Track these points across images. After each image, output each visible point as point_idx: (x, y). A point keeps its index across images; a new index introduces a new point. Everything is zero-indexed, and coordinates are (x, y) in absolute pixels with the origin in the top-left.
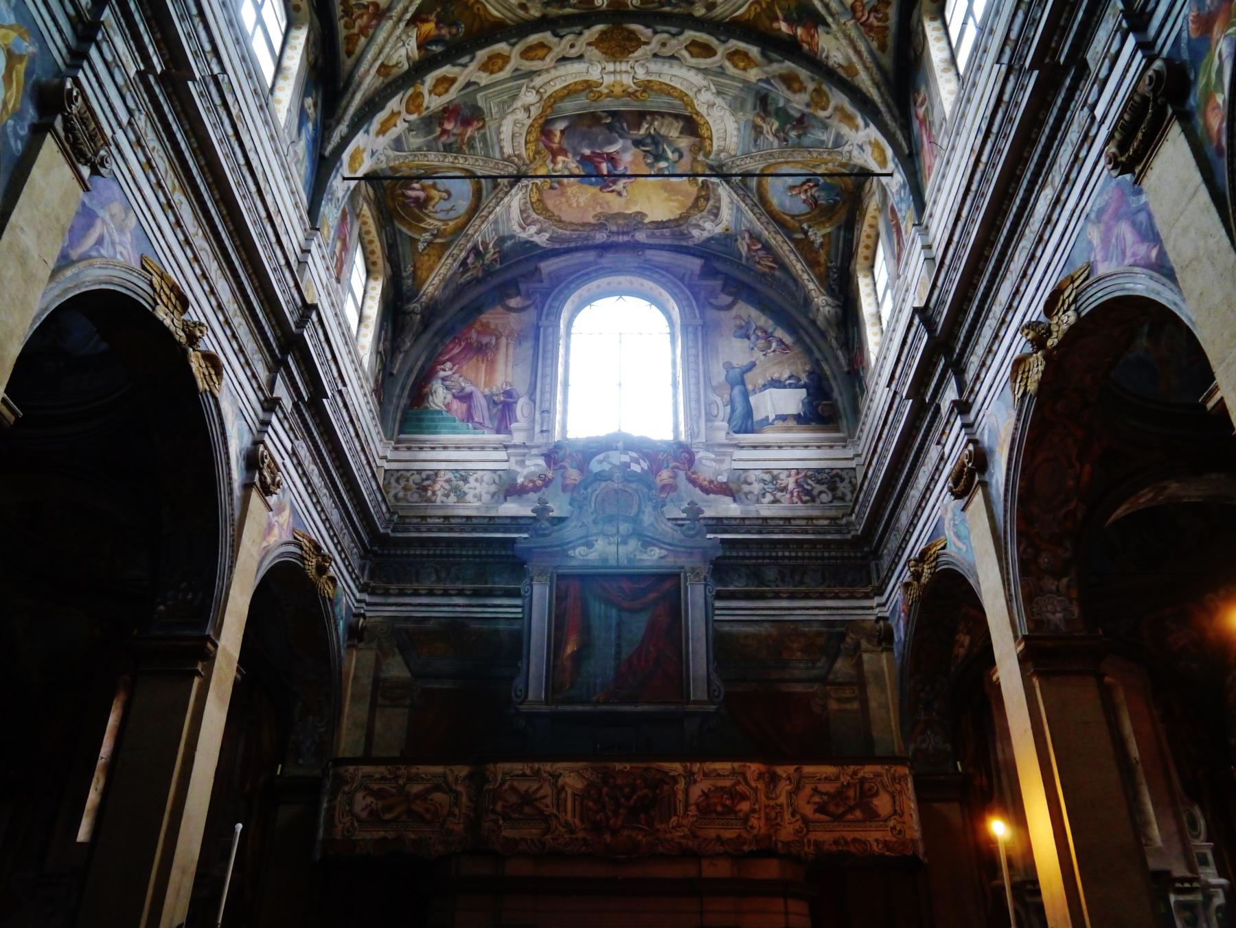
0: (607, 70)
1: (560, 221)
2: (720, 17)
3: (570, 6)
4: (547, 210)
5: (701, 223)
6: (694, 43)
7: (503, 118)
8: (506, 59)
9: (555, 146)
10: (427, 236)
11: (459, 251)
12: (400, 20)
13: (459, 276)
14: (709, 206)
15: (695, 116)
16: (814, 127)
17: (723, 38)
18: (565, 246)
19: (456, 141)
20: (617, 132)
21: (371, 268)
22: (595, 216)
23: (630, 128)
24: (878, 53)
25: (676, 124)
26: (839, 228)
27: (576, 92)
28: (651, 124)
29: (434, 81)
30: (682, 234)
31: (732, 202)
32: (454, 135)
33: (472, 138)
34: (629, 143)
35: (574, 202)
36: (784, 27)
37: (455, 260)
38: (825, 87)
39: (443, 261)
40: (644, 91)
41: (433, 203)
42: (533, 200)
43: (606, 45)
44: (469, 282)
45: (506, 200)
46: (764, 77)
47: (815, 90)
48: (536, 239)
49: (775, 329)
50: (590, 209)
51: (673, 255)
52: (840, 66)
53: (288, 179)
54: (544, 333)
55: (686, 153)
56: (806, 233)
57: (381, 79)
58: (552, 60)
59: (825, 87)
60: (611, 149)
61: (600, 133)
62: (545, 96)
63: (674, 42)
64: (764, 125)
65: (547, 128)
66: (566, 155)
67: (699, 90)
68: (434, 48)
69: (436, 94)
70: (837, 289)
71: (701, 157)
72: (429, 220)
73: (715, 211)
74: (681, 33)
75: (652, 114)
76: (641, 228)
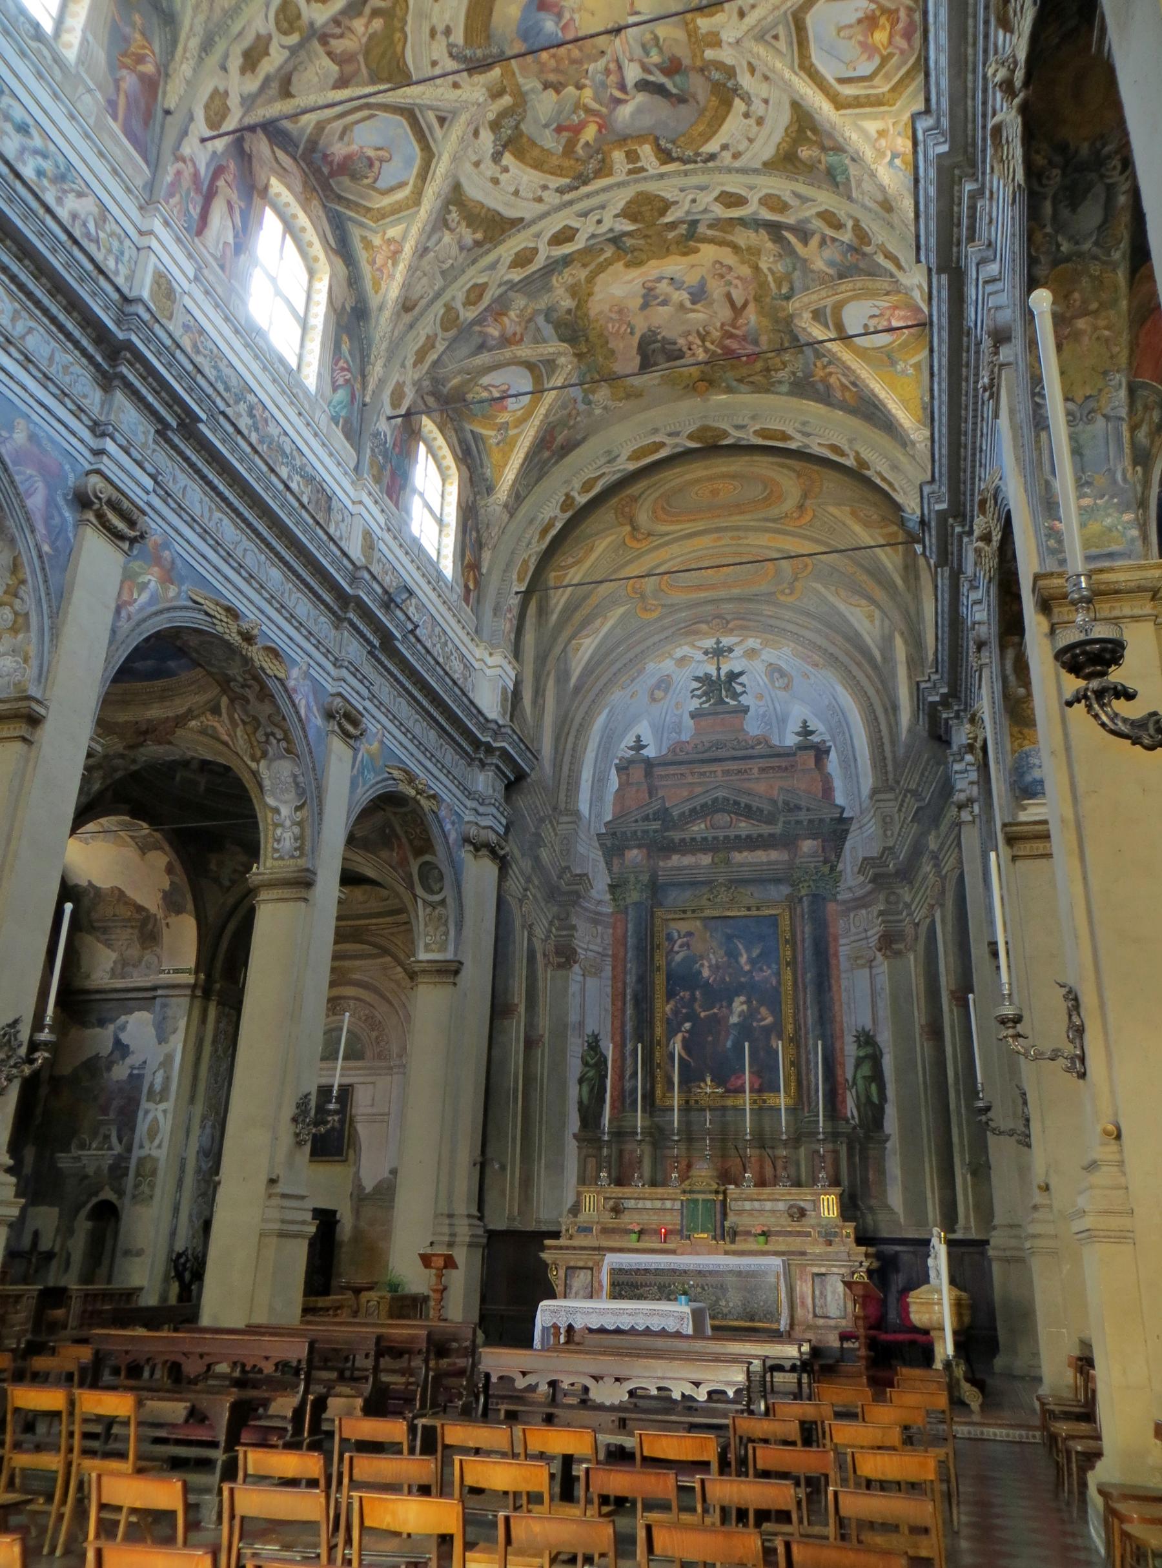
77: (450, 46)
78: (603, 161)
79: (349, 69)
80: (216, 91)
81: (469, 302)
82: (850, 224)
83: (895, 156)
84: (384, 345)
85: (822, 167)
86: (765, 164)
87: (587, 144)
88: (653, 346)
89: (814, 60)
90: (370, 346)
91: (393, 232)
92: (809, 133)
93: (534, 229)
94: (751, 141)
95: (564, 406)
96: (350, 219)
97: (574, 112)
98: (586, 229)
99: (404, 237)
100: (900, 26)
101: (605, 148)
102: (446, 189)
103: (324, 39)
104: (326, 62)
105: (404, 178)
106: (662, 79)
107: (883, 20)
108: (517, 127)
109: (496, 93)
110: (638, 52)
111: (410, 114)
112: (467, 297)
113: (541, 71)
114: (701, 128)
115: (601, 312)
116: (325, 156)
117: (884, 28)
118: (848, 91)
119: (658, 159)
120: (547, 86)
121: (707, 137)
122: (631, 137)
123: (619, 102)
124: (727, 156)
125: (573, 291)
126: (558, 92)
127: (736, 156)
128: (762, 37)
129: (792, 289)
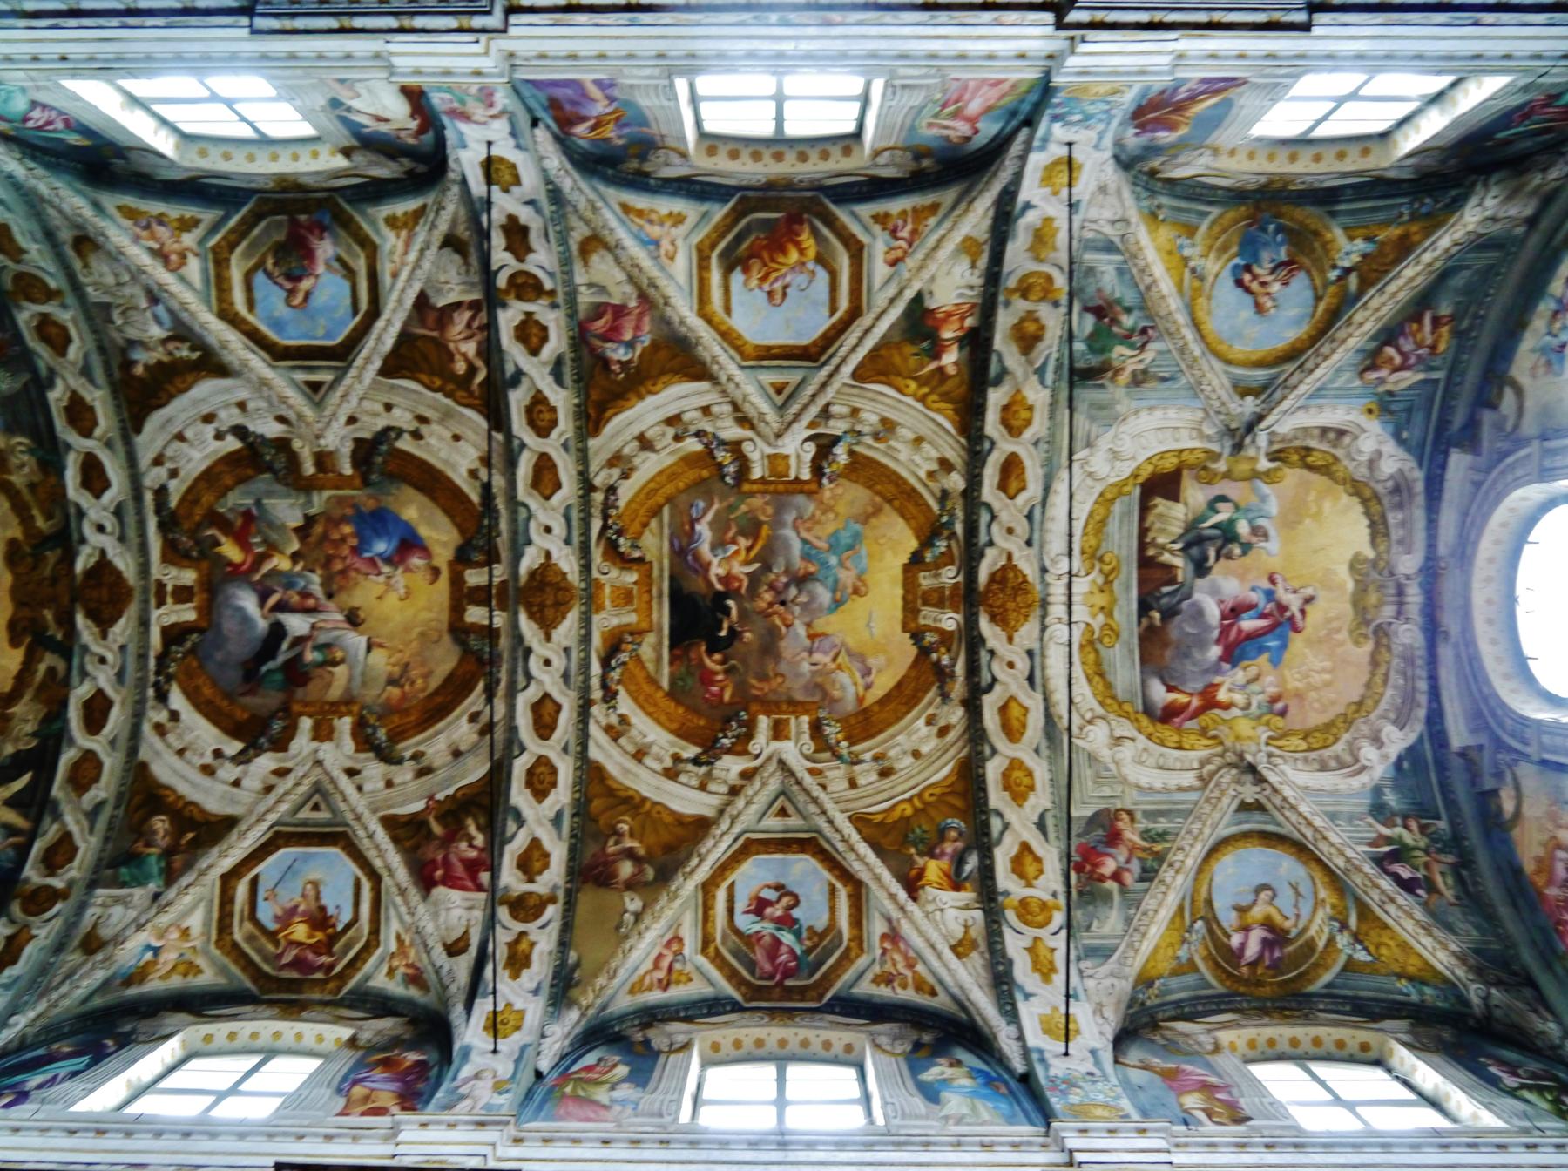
1: (1360, 704)
2: (963, 453)
3: (954, 665)
4: (1328, 727)
5: (1364, 458)
6: (1003, 486)
7: (1124, 781)
8: (1015, 764)
9: (1196, 702)
10: (1343, 940)
11: (1379, 888)
12: (902, 909)
14: (1325, 447)
15: (1140, 480)
16: (1099, 290)
17: (987, 445)
18: (1423, 699)
19: (1140, 859)
20: (1180, 602)
21: (1372, 1055)
22: (1357, 643)
23: (1172, 581)
24: (942, 212)
25: (1160, 509)
26: (1333, 214)
27: (1098, 663)
28: (1163, 548)
29: (1015, 877)
30: (1397, 490)
32: (1128, 862)
33: (1146, 835)
34: (1200, 582)
35: (1316, 679)
36: (950, 358)
37: (1392, 900)
38: (1012, 283)
39: (1390, 922)
40: (1101, 560)
41: (1278, 919)
42: (1304, 746)
44: (1460, 881)
45: (1288, 792)
46: (1034, 378)
49: (1552, 296)
50: (1339, 650)
52: (973, 266)
53: (927, 1144)
55: (1217, 490)
56: (1348, 271)
57: (975, 955)
58: (1030, 697)
59: (1012, 283)
60: (1213, 613)
61: (1180, 628)
62: (1100, 710)
63: (1004, 516)
65: (1159, 713)
66: (1217, 686)
67: (1090, 474)
68: (968, 868)
69: (1036, 878)
70: (1453, 193)
71: (1221, 466)
72: (1312, 932)
73: (1332, 435)
75: (1142, 547)
76: (1388, 563)
77: (400, 432)
79: (431, 318)
80: (517, 181)
81: (45, 323)
82: (57, 883)
83: (156, 951)
84: (43, 189)
85: (140, 847)
86: (144, 767)
87: (219, 544)
89: (283, 851)
90: (47, 166)
91: (194, 268)
92: (190, 835)
93: (119, 445)
98: (97, 510)
99: (183, 280)
100: (310, 956)
101: (205, 565)
102: (228, 358)
103: (474, 306)
104: (452, 298)
105: (259, 308)
107: (320, 936)
108: (269, 468)
110: (322, 638)
111: (343, 353)
112: (55, 324)
114: (207, 691)
117: (310, 937)
118: (242, 890)
119: (174, 625)
120: (310, 521)
121: (193, 696)
123: (263, 600)
124: (162, 716)
126: (297, 530)
127: (160, 729)
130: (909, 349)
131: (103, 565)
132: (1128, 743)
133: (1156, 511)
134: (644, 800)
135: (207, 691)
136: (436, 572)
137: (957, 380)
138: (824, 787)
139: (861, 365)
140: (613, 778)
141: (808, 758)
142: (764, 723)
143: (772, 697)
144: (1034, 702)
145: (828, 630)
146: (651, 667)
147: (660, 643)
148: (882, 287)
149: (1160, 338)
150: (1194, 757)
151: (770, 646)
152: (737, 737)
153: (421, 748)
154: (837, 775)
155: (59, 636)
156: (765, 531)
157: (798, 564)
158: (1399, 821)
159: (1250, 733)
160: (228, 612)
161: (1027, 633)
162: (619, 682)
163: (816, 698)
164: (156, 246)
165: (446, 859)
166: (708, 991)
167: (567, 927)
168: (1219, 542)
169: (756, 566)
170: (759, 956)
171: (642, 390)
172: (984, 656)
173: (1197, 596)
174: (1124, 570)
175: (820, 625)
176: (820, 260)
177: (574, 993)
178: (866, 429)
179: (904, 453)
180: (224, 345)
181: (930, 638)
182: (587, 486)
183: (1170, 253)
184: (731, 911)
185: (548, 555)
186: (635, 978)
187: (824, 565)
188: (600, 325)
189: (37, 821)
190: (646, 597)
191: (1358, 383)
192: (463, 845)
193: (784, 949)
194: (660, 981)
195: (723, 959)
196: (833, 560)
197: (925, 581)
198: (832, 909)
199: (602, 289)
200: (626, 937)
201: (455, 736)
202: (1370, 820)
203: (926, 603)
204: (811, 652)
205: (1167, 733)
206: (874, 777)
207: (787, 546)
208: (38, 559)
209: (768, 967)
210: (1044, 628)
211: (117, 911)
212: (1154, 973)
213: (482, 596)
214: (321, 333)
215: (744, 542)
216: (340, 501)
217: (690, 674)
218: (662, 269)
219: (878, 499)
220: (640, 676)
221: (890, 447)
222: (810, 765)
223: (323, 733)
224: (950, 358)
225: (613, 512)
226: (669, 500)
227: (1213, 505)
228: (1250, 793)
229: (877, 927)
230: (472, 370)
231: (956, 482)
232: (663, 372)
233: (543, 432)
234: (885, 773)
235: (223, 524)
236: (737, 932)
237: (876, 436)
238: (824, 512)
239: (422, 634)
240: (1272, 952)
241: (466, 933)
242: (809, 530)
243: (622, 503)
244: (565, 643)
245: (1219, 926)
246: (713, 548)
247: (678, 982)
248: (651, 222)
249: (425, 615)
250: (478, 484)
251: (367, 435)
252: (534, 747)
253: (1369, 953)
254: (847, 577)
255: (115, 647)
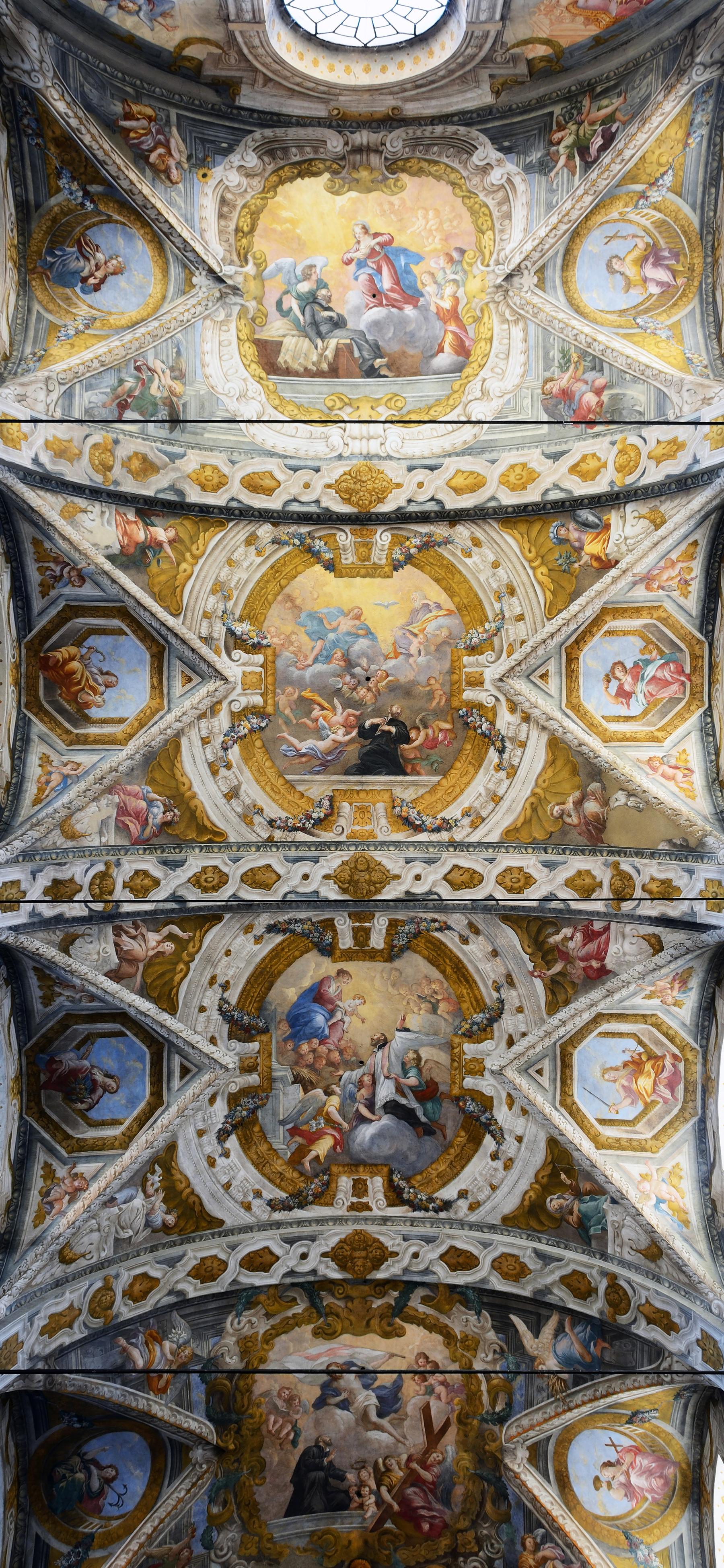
0: (379, 441)
2: (241, 526)
5: (245, 181)
7: (518, 386)
8: (504, 480)
9: (452, 327)
13: (619, 115)
14: (235, 215)
15: (263, 375)
16: (104, 406)
17: (234, 504)
18: (451, 129)
20: (367, 341)
22: (402, 188)
23: (349, 347)
24: (40, 537)
30: (271, 153)
31: (202, 232)
32: (586, 383)
33: (563, 368)
34: (350, 325)
35: (433, 223)
39: (639, 154)
41: (636, 253)
42: (490, 233)
43: (378, 484)
44: (605, 92)
45: (529, 246)
47: (110, 468)
48: (494, 155)
51: (285, 110)
54: (494, 12)
55: (272, 309)
56: (86, 194)
60: (377, 313)
64: (171, 383)
65: (461, 358)
68: (591, 518)
69: (599, 459)
70: (19, 98)
71: (252, 305)
72: (648, 224)
73: (225, 209)
74: (287, 503)
75: (320, 374)
76: (334, 161)
77: (223, 1000)
78: (327, 1184)
79: (127, 969)
80: (16, 883)
82: (603, 1285)
83: (660, 1201)
85: (573, 1219)
86: (505, 1219)
87: (317, 1157)
88: (313, 1475)
92: (563, 1176)
93: (232, 1239)
94: (494, 1188)
95: (176, 1536)
96: (43, 1141)
97: (315, 1118)
99: (95, 1177)
100: (665, 1074)
101: (335, 1169)
102: (161, 1141)
103: (118, 931)
104: (111, 950)
105: (120, 1117)
106: (414, 1105)
107: (648, 1067)
108: (253, 1111)
109: (247, 1068)
110: (398, 1070)
112: (131, 1285)
113: (297, 1063)
114: (442, 1167)
115: (266, 1394)
116: (52, 1061)
117: (649, 1075)
120: (297, 1080)
121: (445, 1180)
122: (365, 1164)
123: (363, 1120)
124: (463, 1204)
125: (246, 1346)
126: (306, 1091)
127: (472, 1208)
128: (526, 1070)
129: (509, 1405)
130: (154, 568)
131: (336, 1255)
132: (487, 384)
133: (290, 361)
134: (533, 794)
135: (442, 1167)
136: (341, 973)
137: (179, 528)
138: (523, 642)
139: (166, 608)
140: (517, 819)
141: (498, 658)
142: (469, 694)
143: (447, 688)
144: (452, 465)
145: (391, 640)
146: (422, 791)
147: (401, 782)
148: (103, 590)
149: (143, 355)
150: (498, 328)
151: (405, 691)
152: (481, 716)
153: (490, 983)
154: (514, 631)
155: (396, 1294)
156: (307, 694)
157: (336, 665)
158: (554, 148)
159: (478, 279)
160: (375, 1150)
161: (394, 471)
162: (435, 818)
163: (449, 650)
164: (67, 1197)
165: (583, 959)
166: (695, 737)
167: (639, 853)
168: (317, 308)
169: (336, 701)
170: (666, 694)
171: (188, 794)
172: (413, 508)
173: (362, 327)
174: (340, 389)
175: (386, 647)
176: (79, 644)
177: (692, 843)
178: (221, 607)
179: (241, 575)
180: (150, 1145)
181: (398, 555)
182: (269, 843)
183: (72, 346)
184: (628, 719)
185: (327, 877)
186: (682, 795)
187: (335, 644)
188: (134, 828)
189: (551, 1307)
190: (362, 795)
191: (180, 185)
192: (571, 944)
193: (659, 674)
194: (685, 776)
195: (667, 724)
196: (332, 636)
197: (349, 558)
198: (626, 633)
199: (104, 823)
200: (647, 802)
201: (480, 955)
202: (552, 174)
203: (368, 559)
204: (411, 655)
205: (477, 351)
206: (515, 599)
207: (320, 674)
208: (330, 1312)
209: (675, 687)
210: (390, 457)
211: (626, 1233)
212: (680, 358)
213: (361, 935)
214: (139, 1065)
215: (317, 712)
216: (281, 1053)
217: (427, 758)
218: (87, 773)
219: (279, 598)
220: (429, 799)
221: (236, 588)
222: (504, 655)
223: (477, 1068)
224: (161, 533)
225: (291, 823)
226: (281, 775)
227: (285, 313)
228: (528, 280)
229: (641, 593)
230: (171, 937)
231: (265, 531)
232: (173, 776)
233: (223, 879)
234: (512, 592)
235: (300, 1153)
236: (645, 713)
237: (227, 598)
238: (291, 643)
239: (394, 985)
240: (665, 258)
241: (643, 937)
242: (306, 657)
243: (284, 815)
244: (402, 862)
245: (641, 304)
246: (322, 738)
247: (686, 761)
248: (48, 782)
249: (377, 982)
250: (267, 936)
251: (226, 1027)
252: (489, 888)
253: (665, 173)
254: (346, 624)
255: (405, 1244)
